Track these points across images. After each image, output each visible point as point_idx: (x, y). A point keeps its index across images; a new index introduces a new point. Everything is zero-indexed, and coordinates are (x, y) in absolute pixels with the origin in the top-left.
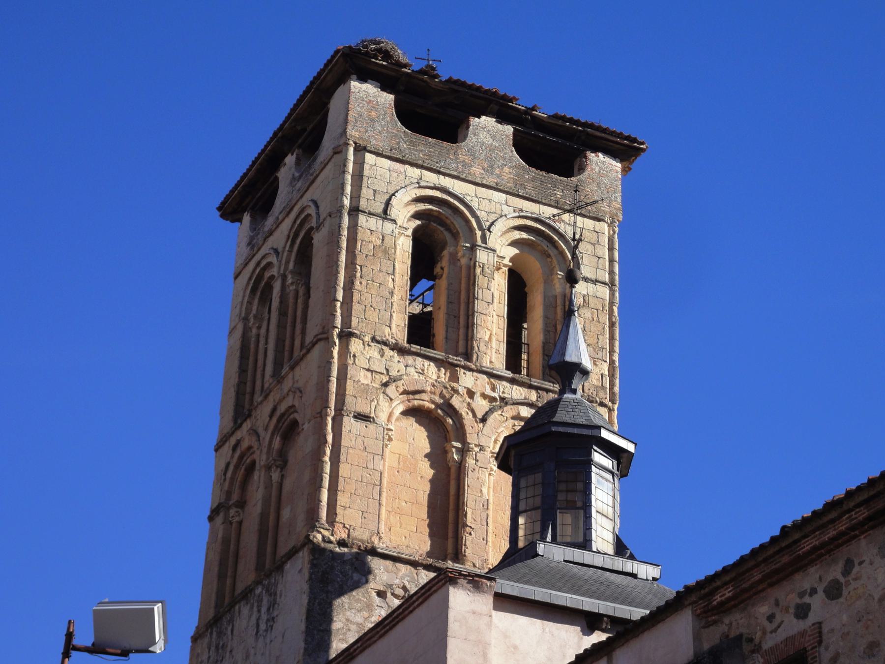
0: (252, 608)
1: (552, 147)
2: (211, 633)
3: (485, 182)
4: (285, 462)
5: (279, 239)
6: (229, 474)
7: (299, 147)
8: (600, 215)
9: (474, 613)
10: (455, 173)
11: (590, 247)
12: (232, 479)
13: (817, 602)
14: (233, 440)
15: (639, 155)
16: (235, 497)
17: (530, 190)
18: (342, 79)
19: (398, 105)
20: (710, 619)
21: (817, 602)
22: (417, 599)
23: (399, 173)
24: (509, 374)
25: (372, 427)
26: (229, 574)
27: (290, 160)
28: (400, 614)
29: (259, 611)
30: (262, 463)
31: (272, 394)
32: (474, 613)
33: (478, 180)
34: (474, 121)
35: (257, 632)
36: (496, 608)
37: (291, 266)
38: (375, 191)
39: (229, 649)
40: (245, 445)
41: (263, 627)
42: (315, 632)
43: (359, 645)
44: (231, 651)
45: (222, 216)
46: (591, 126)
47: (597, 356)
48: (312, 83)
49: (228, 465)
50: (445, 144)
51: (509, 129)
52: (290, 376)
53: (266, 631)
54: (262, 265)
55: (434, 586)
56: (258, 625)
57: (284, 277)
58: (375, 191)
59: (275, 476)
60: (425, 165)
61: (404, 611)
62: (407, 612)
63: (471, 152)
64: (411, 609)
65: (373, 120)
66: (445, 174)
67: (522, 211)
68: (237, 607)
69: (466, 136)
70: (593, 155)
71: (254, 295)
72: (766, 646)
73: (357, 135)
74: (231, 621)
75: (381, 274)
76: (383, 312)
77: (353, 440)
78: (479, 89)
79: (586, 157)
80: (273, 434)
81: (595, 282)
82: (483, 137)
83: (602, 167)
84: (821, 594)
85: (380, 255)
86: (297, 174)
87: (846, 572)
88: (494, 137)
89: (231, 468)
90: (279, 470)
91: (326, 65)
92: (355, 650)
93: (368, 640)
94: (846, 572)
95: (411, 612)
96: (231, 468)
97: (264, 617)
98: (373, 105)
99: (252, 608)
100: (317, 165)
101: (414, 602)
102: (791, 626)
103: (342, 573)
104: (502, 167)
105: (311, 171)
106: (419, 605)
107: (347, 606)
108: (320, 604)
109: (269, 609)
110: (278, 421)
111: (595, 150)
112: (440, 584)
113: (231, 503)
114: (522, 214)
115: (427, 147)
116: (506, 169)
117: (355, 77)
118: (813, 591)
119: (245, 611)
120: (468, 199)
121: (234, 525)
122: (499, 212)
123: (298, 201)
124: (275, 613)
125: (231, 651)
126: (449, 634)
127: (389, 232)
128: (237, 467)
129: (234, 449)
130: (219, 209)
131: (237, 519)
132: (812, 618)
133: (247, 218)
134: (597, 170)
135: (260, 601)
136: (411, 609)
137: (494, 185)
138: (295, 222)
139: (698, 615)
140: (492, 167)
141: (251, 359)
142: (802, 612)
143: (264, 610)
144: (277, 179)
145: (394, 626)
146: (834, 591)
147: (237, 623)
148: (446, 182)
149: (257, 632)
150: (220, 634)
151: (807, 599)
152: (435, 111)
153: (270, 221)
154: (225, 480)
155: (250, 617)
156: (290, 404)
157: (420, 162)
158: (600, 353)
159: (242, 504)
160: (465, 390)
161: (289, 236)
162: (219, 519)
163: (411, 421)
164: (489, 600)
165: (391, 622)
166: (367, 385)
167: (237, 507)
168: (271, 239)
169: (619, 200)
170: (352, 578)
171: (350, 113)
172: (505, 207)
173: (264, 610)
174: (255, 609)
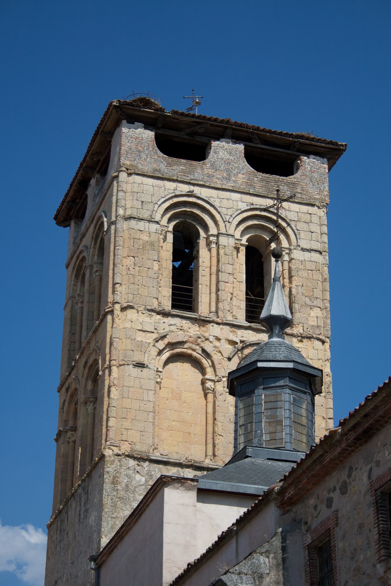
0: (77, 503)
1: (273, 156)
2: (58, 521)
3: (224, 187)
4: (96, 398)
5: (87, 240)
6: (65, 409)
7: (98, 172)
8: (312, 202)
9: (183, 505)
10: (201, 183)
11: (305, 225)
12: (68, 411)
13: (336, 495)
14: (66, 385)
15: (342, 154)
16: (71, 424)
17: (259, 189)
18: (117, 124)
19: (157, 137)
20: (286, 509)
21: (336, 495)
22: (150, 497)
23: (159, 187)
24: (248, 324)
25: (145, 370)
26: (69, 478)
27: (93, 182)
28: (142, 507)
29: (80, 505)
30: (81, 400)
31: (85, 351)
32: (183, 505)
33: (219, 186)
34: (215, 144)
35: (80, 520)
36: (198, 501)
37: (96, 257)
38: (142, 202)
39: (66, 532)
40: (73, 387)
41: (82, 517)
42: (110, 519)
43: (124, 529)
44: (67, 534)
45: (57, 223)
46: (302, 137)
47: (313, 304)
48: (98, 128)
49: (65, 401)
50: (194, 163)
51: (241, 147)
52: (94, 338)
53: (84, 519)
54: (80, 258)
55: (157, 486)
56: (80, 515)
57: (91, 267)
58: (142, 202)
59: (90, 408)
60: (179, 179)
61: (144, 505)
62: (145, 506)
63: (213, 165)
64: (147, 503)
65: (140, 151)
66: (194, 185)
67: (252, 204)
68: (70, 502)
69: (208, 156)
70: (305, 158)
71: (78, 279)
72: (313, 527)
73: (128, 163)
74: (67, 513)
75: (149, 261)
76: (151, 289)
77: (133, 381)
78: (216, 120)
79: (300, 160)
80: (87, 379)
81: (310, 250)
82: (222, 154)
83: (311, 167)
84: (338, 490)
85: (148, 247)
86: (97, 192)
87: (349, 476)
88: (230, 154)
89: (66, 404)
90: (92, 404)
91: (105, 115)
92: (123, 533)
93: (128, 525)
94: (349, 476)
95: (148, 505)
96: (66, 404)
97: (83, 509)
98: (139, 141)
99: (77, 503)
100: (106, 186)
101: (148, 499)
102: (325, 513)
103: (127, 476)
104: (236, 175)
105: (103, 191)
106: (151, 501)
107: (132, 499)
108: (112, 500)
109: (85, 504)
110: (89, 370)
111: (308, 154)
112: (160, 486)
113: (67, 428)
114: (252, 207)
115: (180, 166)
116: (240, 176)
117: (124, 122)
118: (335, 489)
119: (74, 505)
120: (211, 201)
121: (71, 443)
122: (235, 207)
123: (97, 212)
124: (88, 506)
125: (67, 534)
126: (165, 520)
127: (154, 230)
128: (70, 403)
129: (67, 390)
130: (56, 218)
131: (73, 439)
132: (333, 508)
133: (73, 224)
134: (309, 169)
135: (80, 498)
136: (147, 503)
137: (231, 188)
138: (95, 227)
139: (279, 507)
140: (229, 175)
141: (78, 325)
142: (329, 503)
143: (83, 504)
144: (87, 195)
145: (140, 515)
146: (344, 490)
147: (70, 514)
149: (80, 520)
150: (62, 521)
151: (332, 495)
152: (184, 140)
153: (83, 227)
154: (63, 412)
155: (76, 508)
156: (94, 358)
157: (175, 178)
158: (315, 302)
159: (74, 429)
160: (214, 338)
161: (93, 237)
162: (61, 440)
163: (171, 366)
164: (193, 495)
165: (138, 512)
166: (142, 341)
167: (71, 430)
168: (84, 239)
169: (327, 188)
170: (135, 478)
171: (123, 148)
172: (240, 203)
173: (83, 504)
174: (78, 504)
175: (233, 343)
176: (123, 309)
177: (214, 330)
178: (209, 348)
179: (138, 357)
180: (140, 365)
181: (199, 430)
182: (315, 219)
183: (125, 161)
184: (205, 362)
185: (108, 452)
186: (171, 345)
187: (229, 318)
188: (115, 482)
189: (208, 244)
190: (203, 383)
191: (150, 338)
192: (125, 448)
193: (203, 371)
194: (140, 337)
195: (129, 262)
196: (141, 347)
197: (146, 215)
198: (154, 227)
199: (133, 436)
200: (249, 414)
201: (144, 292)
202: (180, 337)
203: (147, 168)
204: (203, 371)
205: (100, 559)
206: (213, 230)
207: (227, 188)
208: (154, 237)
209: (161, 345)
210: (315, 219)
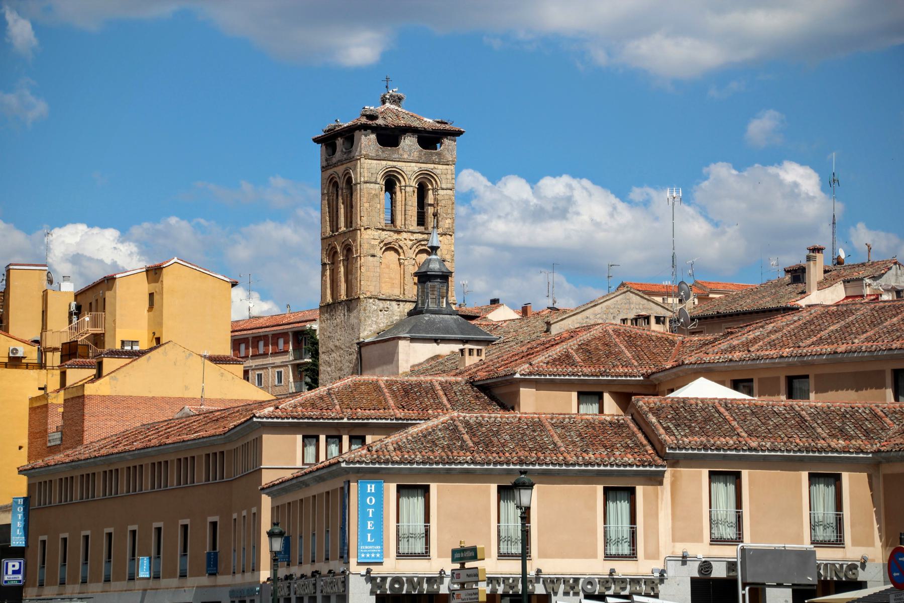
148: (395, 164)
152: (389, 137)
175: (411, 240)
176: (365, 229)
177: (404, 235)
178: (401, 243)
179: (372, 252)
180: (373, 256)
181: (397, 282)
182: (449, 172)
183: (363, 152)
184: (400, 251)
185: (361, 297)
186: (386, 245)
187: (411, 229)
188: (365, 310)
189: (401, 190)
190: (399, 259)
191: (376, 242)
192: (368, 294)
193: (399, 254)
194: (373, 242)
195: (367, 205)
196: (373, 246)
197: (373, 180)
198: (377, 186)
199: (372, 288)
200: (423, 292)
201: (374, 220)
202: (390, 240)
203: (373, 154)
204: (399, 254)
205: (361, 345)
206: (403, 184)
207: (409, 159)
208: (377, 192)
209: (382, 245)
210: (449, 172)
